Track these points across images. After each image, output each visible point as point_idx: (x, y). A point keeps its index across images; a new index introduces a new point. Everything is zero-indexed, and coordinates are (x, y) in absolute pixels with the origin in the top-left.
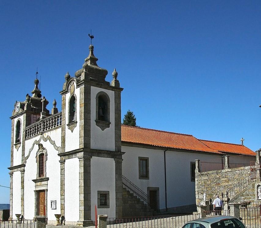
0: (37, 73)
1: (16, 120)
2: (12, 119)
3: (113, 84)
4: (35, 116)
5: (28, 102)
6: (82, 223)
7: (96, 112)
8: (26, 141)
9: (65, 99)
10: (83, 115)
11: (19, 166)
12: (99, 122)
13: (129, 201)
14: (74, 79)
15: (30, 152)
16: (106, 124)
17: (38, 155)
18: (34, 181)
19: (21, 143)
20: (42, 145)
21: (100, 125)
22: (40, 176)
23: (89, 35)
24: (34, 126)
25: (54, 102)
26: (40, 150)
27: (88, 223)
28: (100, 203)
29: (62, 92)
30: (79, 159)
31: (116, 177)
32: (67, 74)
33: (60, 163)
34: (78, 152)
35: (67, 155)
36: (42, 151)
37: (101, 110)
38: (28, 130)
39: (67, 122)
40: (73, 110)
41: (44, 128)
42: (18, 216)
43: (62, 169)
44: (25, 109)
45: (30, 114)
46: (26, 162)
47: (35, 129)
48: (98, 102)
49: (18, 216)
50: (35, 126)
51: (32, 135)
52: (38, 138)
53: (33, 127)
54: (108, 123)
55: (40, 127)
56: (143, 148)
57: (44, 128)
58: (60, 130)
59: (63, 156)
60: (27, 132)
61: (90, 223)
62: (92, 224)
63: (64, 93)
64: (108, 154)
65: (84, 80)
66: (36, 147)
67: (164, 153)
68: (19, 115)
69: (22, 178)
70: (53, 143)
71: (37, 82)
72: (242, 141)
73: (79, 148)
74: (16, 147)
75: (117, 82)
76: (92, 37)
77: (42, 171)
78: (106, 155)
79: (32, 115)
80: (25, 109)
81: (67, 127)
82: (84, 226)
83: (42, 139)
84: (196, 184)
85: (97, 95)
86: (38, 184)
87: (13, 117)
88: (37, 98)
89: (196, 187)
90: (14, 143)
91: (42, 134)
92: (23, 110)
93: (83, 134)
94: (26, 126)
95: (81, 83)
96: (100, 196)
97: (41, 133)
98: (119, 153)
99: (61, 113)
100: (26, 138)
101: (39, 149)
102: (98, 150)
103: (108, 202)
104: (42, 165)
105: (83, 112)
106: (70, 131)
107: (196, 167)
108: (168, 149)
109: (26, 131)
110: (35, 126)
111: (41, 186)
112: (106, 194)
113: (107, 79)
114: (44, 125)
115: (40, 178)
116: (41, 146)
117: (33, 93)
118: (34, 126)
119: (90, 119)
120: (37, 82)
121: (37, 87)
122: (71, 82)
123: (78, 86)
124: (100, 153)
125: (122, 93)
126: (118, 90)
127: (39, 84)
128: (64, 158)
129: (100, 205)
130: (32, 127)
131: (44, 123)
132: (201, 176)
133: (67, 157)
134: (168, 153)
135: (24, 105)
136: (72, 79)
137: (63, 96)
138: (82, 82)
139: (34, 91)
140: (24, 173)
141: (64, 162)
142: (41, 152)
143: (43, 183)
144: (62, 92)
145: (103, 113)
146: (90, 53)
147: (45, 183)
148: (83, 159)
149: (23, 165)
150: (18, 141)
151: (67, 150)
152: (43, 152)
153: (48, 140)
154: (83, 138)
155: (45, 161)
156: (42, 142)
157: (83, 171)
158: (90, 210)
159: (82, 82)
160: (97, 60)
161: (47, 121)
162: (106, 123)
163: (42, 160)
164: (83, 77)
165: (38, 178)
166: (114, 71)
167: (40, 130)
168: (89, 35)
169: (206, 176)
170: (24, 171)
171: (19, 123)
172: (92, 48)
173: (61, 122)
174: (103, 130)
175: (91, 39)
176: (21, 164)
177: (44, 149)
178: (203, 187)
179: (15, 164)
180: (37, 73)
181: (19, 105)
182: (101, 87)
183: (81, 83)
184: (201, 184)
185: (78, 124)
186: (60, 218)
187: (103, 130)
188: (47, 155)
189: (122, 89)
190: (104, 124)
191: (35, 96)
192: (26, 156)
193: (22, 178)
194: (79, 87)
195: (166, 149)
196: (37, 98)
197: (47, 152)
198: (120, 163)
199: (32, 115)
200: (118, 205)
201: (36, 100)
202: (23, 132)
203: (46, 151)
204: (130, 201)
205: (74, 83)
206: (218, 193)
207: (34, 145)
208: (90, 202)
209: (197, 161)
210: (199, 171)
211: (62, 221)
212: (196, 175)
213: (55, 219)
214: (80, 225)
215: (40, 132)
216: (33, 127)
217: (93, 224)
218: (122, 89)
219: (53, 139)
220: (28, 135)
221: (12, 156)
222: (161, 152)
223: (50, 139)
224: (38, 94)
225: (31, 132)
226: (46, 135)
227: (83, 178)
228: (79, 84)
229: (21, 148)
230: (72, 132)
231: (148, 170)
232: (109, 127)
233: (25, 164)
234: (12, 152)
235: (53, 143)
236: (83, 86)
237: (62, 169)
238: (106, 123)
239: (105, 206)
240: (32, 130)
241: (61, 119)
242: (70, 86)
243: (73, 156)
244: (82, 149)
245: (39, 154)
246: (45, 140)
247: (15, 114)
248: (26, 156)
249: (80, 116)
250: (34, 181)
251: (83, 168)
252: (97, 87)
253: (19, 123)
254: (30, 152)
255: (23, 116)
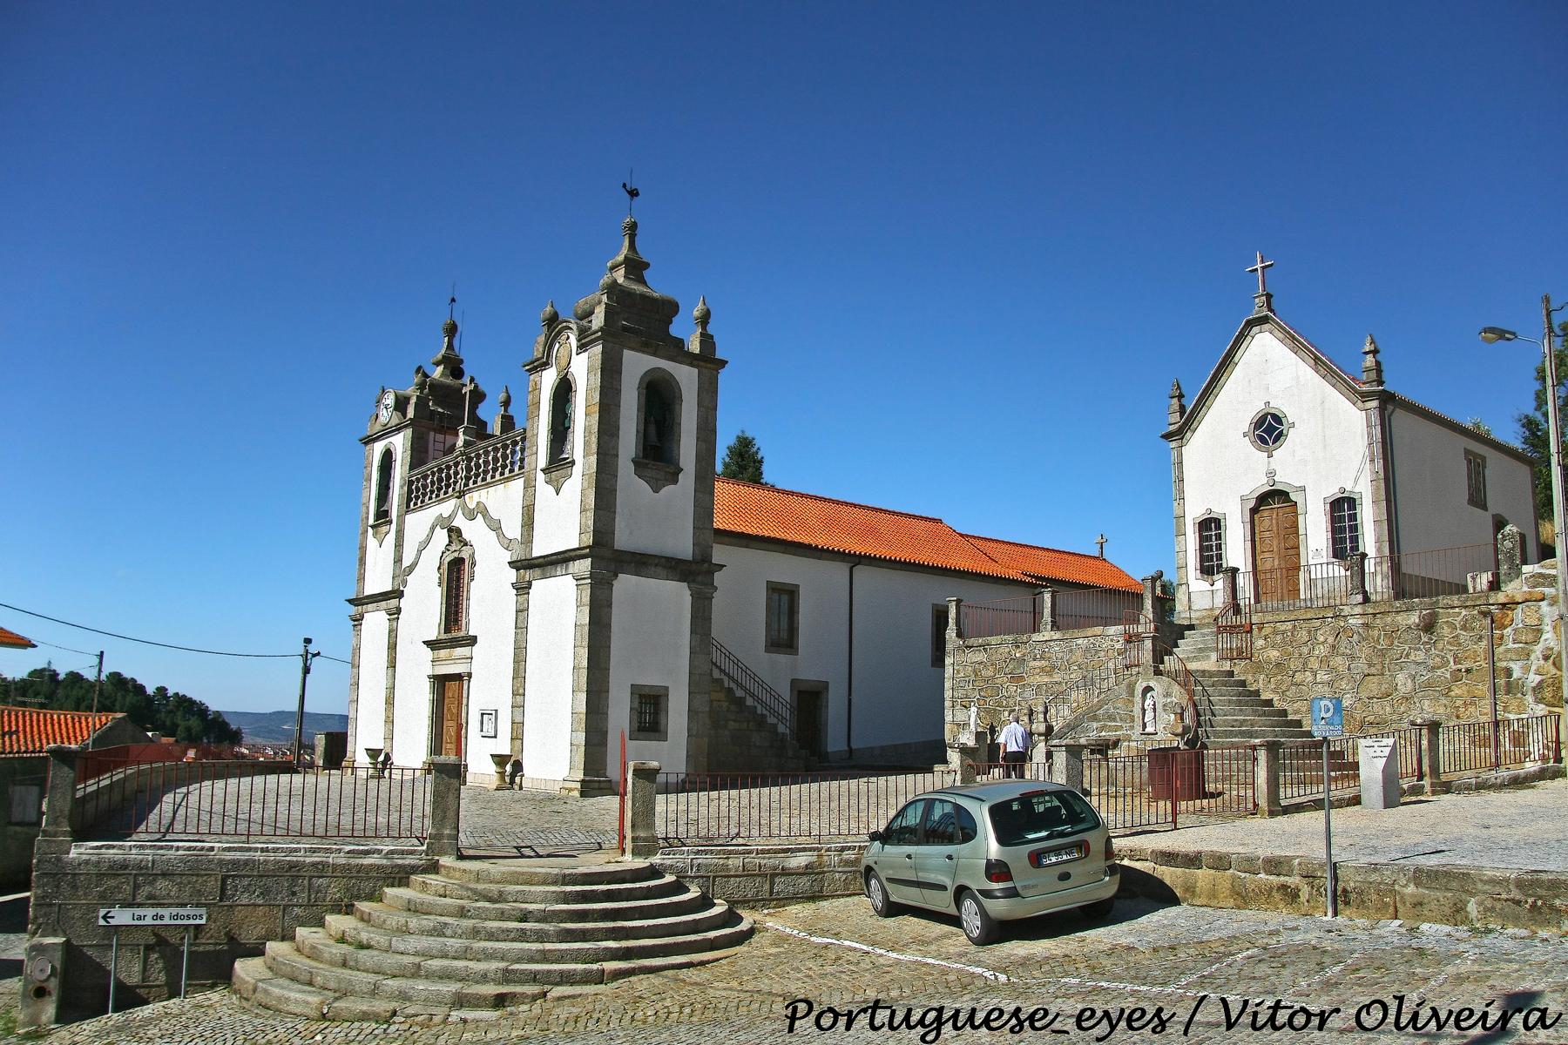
1: (379, 448)
2: (366, 443)
3: (694, 346)
4: (440, 437)
6: (578, 785)
9: (537, 388)
10: (594, 439)
12: (645, 466)
13: (732, 723)
15: (420, 552)
17: (446, 562)
19: (391, 522)
20: (458, 531)
22: (447, 630)
23: (624, 186)
24: (436, 469)
25: (502, 396)
26: (453, 547)
27: (596, 785)
30: (577, 580)
31: (693, 643)
33: (515, 591)
34: (574, 559)
37: (652, 429)
39: (542, 461)
41: (467, 478)
42: (373, 753)
43: (522, 611)
44: (411, 413)
45: (424, 429)
46: (405, 583)
47: (440, 480)
48: (643, 400)
49: (373, 753)
50: (440, 471)
52: (446, 508)
54: (672, 471)
55: (456, 473)
56: (783, 553)
57: (467, 478)
58: (518, 485)
59: (525, 568)
60: (414, 487)
61: (602, 785)
62: (611, 788)
63: (536, 368)
64: (670, 567)
65: (601, 329)
66: (441, 537)
68: (387, 432)
69: (393, 634)
70: (496, 526)
71: (452, 330)
74: (375, 535)
76: (633, 193)
77: (457, 613)
79: (432, 434)
80: (411, 413)
81: (541, 476)
82: (583, 794)
83: (460, 511)
86: (443, 653)
87: (369, 437)
88: (449, 381)
89: (948, 685)
90: (371, 521)
91: (461, 495)
92: (404, 415)
94: (412, 468)
95: (593, 337)
97: (460, 492)
98: (706, 565)
99: (525, 430)
100: (408, 506)
101: (450, 542)
102: (640, 554)
103: (663, 722)
105: (596, 430)
106: (551, 489)
109: (411, 483)
110: (440, 471)
111: (452, 662)
112: (660, 696)
113: (675, 330)
114: (469, 469)
115: (449, 636)
116: (455, 534)
117: (437, 364)
118: (436, 469)
120: (452, 330)
121: (450, 346)
122: (559, 333)
123: (582, 347)
125: (724, 376)
126: (709, 365)
127: (458, 335)
128: (527, 575)
129: (638, 730)
130: (429, 473)
131: (470, 460)
133: (538, 571)
134: (861, 573)
136: (565, 324)
137: (532, 377)
138: (597, 335)
139: (439, 356)
140: (398, 618)
142: (456, 555)
148: (589, 581)
149: (398, 594)
150: (383, 515)
151: (540, 549)
154: (591, 514)
155: (466, 582)
156: (460, 522)
158: (603, 742)
159: (597, 335)
160: (646, 265)
161: (478, 456)
162: (668, 470)
163: (458, 579)
164: (598, 320)
165: (443, 636)
166: (700, 305)
167: (455, 483)
168: (624, 186)
170: (399, 611)
172: (633, 227)
173: (522, 460)
174: (656, 491)
176: (390, 589)
177: (466, 544)
178: (971, 687)
179: (371, 589)
181: (390, 400)
182: (654, 355)
183: (593, 337)
185: (577, 469)
186: (508, 768)
187: (656, 491)
188: (474, 564)
189: (723, 363)
191: (443, 375)
192: (406, 562)
193: (393, 634)
194: (584, 351)
195: (855, 560)
196: (449, 381)
197: (474, 553)
198: (707, 598)
199: (432, 434)
200: (695, 733)
201: (448, 387)
202: (402, 487)
203: (470, 552)
204: (734, 721)
205: (568, 338)
207: (433, 529)
208: (606, 719)
209: (954, 603)
210: (959, 635)
211: (513, 776)
212: (949, 647)
213: (492, 768)
214: (571, 790)
215: (454, 489)
217: (614, 790)
218: (723, 363)
220: (414, 500)
222: (840, 570)
223: (482, 510)
224: (454, 366)
225: (425, 487)
226: (472, 499)
227: (586, 643)
228: (587, 340)
229: (390, 539)
231: (795, 625)
233: (401, 588)
234: (363, 549)
235: (496, 526)
236: (598, 349)
237: (522, 611)
238: (668, 470)
240: (429, 481)
241: (523, 450)
242: (557, 345)
245: (448, 559)
247: (378, 427)
248: (406, 562)
249: (586, 444)
251: (587, 610)
252: (643, 352)
253: (388, 457)
254: (420, 552)
255: (402, 434)
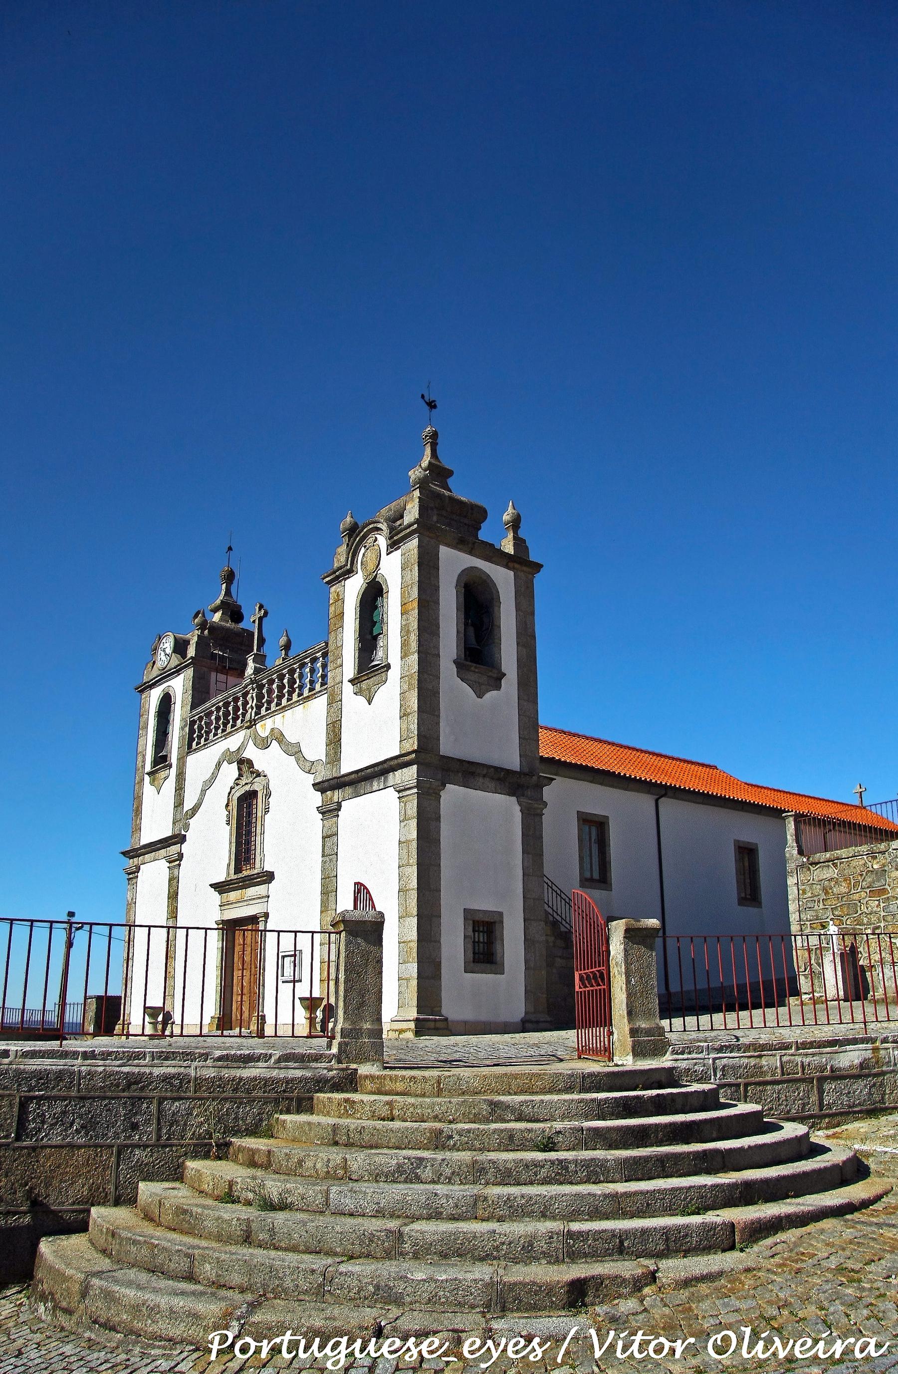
0: (230, 549)
1: (156, 694)
2: (142, 691)
3: (508, 547)
4: (221, 677)
5: (202, 632)
6: (412, 1025)
7: (458, 632)
8: (191, 760)
9: (340, 600)
10: (414, 638)
11: (160, 841)
12: (468, 669)
13: (559, 959)
14: (379, 525)
15: (203, 792)
16: (490, 677)
17: (235, 798)
18: (215, 886)
19: (170, 766)
20: (250, 763)
21: (473, 677)
22: (238, 870)
23: (423, 396)
24: (221, 704)
25: (283, 641)
26: (243, 781)
27: (432, 1025)
28: (471, 956)
29: (333, 576)
30: (399, 792)
31: (526, 864)
32: (348, 519)
33: (320, 816)
34: (393, 769)
35: (350, 784)
36: (252, 783)
37: (471, 630)
38: (201, 719)
39: (349, 668)
40: (371, 632)
41: (259, 707)
42: (151, 1012)
43: (330, 837)
44: (191, 652)
45: (206, 669)
46: (187, 827)
47: (226, 714)
48: (462, 599)
49: (151, 1012)
50: (227, 705)
51: (212, 734)
52: (233, 742)
53: (218, 709)
54: (495, 675)
55: (245, 703)
56: (591, 782)
57: (259, 707)
58: (321, 702)
59: (333, 788)
60: (196, 727)
61: (439, 1025)
62: (447, 1029)
63: (337, 577)
64: (499, 779)
65: (417, 521)
66: (230, 772)
67: (653, 804)
68: (167, 675)
69: (173, 881)
70: (294, 751)
71: (230, 577)
72: (858, 795)
73: (397, 753)
74: (152, 783)
75: (519, 543)
76: (432, 405)
77: (248, 851)
78: (492, 785)
79: (213, 675)
80: (191, 652)
81: (348, 689)
82: (418, 1033)
83: (250, 739)
84: (790, 897)
85: (459, 575)
86: (233, 896)
87: (145, 683)
88: (229, 625)
89: (792, 907)
90: (148, 768)
91: (252, 724)
92: (184, 655)
93: (413, 703)
94: (193, 707)
95: (408, 531)
96: (470, 929)
97: (250, 721)
98: (535, 778)
99: (327, 644)
100: (190, 746)
101: (240, 775)
102: (469, 762)
103: (499, 951)
104: (249, 833)
105: (416, 627)
106: (362, 700)
107: (788, 837)
108: (670, 793)
109: (193, 723)
110: (227, 705)
111: (245, 903)
112: (495, 923)
113: (484, 535)
114: (260, 697)
115: (240, 875)
116: (244, 765)
117: (215, 611)
118: (221, 704)
119: (439, 655)
120: (230, 577)
121: (228, 592)
122: (364, 537)
123: (393, 545)
124: (473, 774)
125: (539, 580)
126: (525, 568)
127: (235, 582)
128: (336, 795)
129: (474, 962)
130: (213, 709)
131: (261, 687)
132: (809, 869)
133: (349, 790)
134: (668, 805)
135: (187, 643)
136: (371, 526)
137: (333, 589)
138: (412, 528)
139: (218, 602)
140: (179, 865)
141: (335, 809)
142: (247, 788)
143: (252, 891)
144: (333, 576)
145: (479, 637)
146: (428, 451)
147: (260, 890)
148: (415, 790)
149: (178, 839)
150: (161, 760)
151: (349, 764)
152: (256, 787)
153: (274, 743)
154: (414, 718)
155: (259, 814)
156: (251, 752)
157: (414, 835)
158: (437, 976)
159: (412, 528)
160: (450, 473)
161: (271, 682)
162: (490, 674)
163: (250, 814)
164: (412, 513)
165: (233, 877)
166: (510, 510)
167: (244, 715)
168: (423, 396)
169: (828, 866)
170: (181, 856)
171: (166, 702)
172: (434, 436)
173: (324, 677)
174: (480, 696)
175: (431, 412)
176: (170, 834)
177: (258, 775)
178: (821, 906)
179: (146, 838)
180: (230, 549)
181: (168, 645)
182: (471, 553)
183: (408, 531)
184: (809, 895)
185: (394, 675)
186: (319, 1014)
187: (480, 696)
188: (268, 795)
189: (538, 567)
190: (485, 678)
191: (221, 619)
192: (188, 805)
193: (173, 881)
194: (396, 550)
195: (660, 791)
196: (229, 625)
197: (268, 784)
198: (537, 815)
199: (213, 675)
200: (532, 965)
201: (228, 630)
202: (182, 728)
203: (264, 783)
204: (560, 957)
205: (376, 540)
206: (882, 925)
207: (219, 765)
208: (440, 948)
209: (791, 819)
210: (801, 852)
211: (324, 1023)
212: (791, 866)
213: (301, 1014)
214: (401, 1031)
215: (242, 721)
216: (218, 709)
217: (451, 1031)
218: (538, 567)
219: (291, 738)
220: (190, 745)
221: (138, 811)
222: (646, 802)
223: (278, 737)
224: (234, 613)
225: (208, 724)
226: (264, 728)
227: (414, 860)
228: (400, 536)
229: (170, 785)
230: (370, 704)
231: (607, 859)
232: (498, 687)
233: (183, 833)
234: (138, 799)
235: (294, 751)
236: (413, 544)
237: (330, 837)
238: (490, 674)
239: (488, 966)
240: (213, 718)
241: (324, 666)
242: (363, 550)
243: (372, 786)
244: (414, 755)
245: (238, 794)
246: (264, 744)
247: (155, 672)
248: (188, 805)
249: (405, 645)
250: (215, 886)
251: (413, 823)
252: (460, 550)
253: (166, 702)
254: (203, 792)
255: (182, 676)
